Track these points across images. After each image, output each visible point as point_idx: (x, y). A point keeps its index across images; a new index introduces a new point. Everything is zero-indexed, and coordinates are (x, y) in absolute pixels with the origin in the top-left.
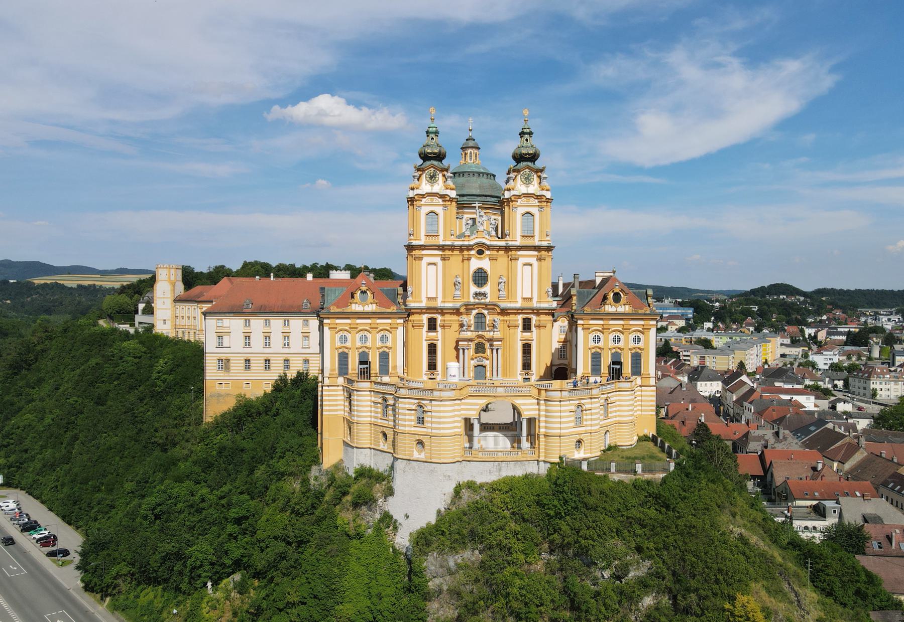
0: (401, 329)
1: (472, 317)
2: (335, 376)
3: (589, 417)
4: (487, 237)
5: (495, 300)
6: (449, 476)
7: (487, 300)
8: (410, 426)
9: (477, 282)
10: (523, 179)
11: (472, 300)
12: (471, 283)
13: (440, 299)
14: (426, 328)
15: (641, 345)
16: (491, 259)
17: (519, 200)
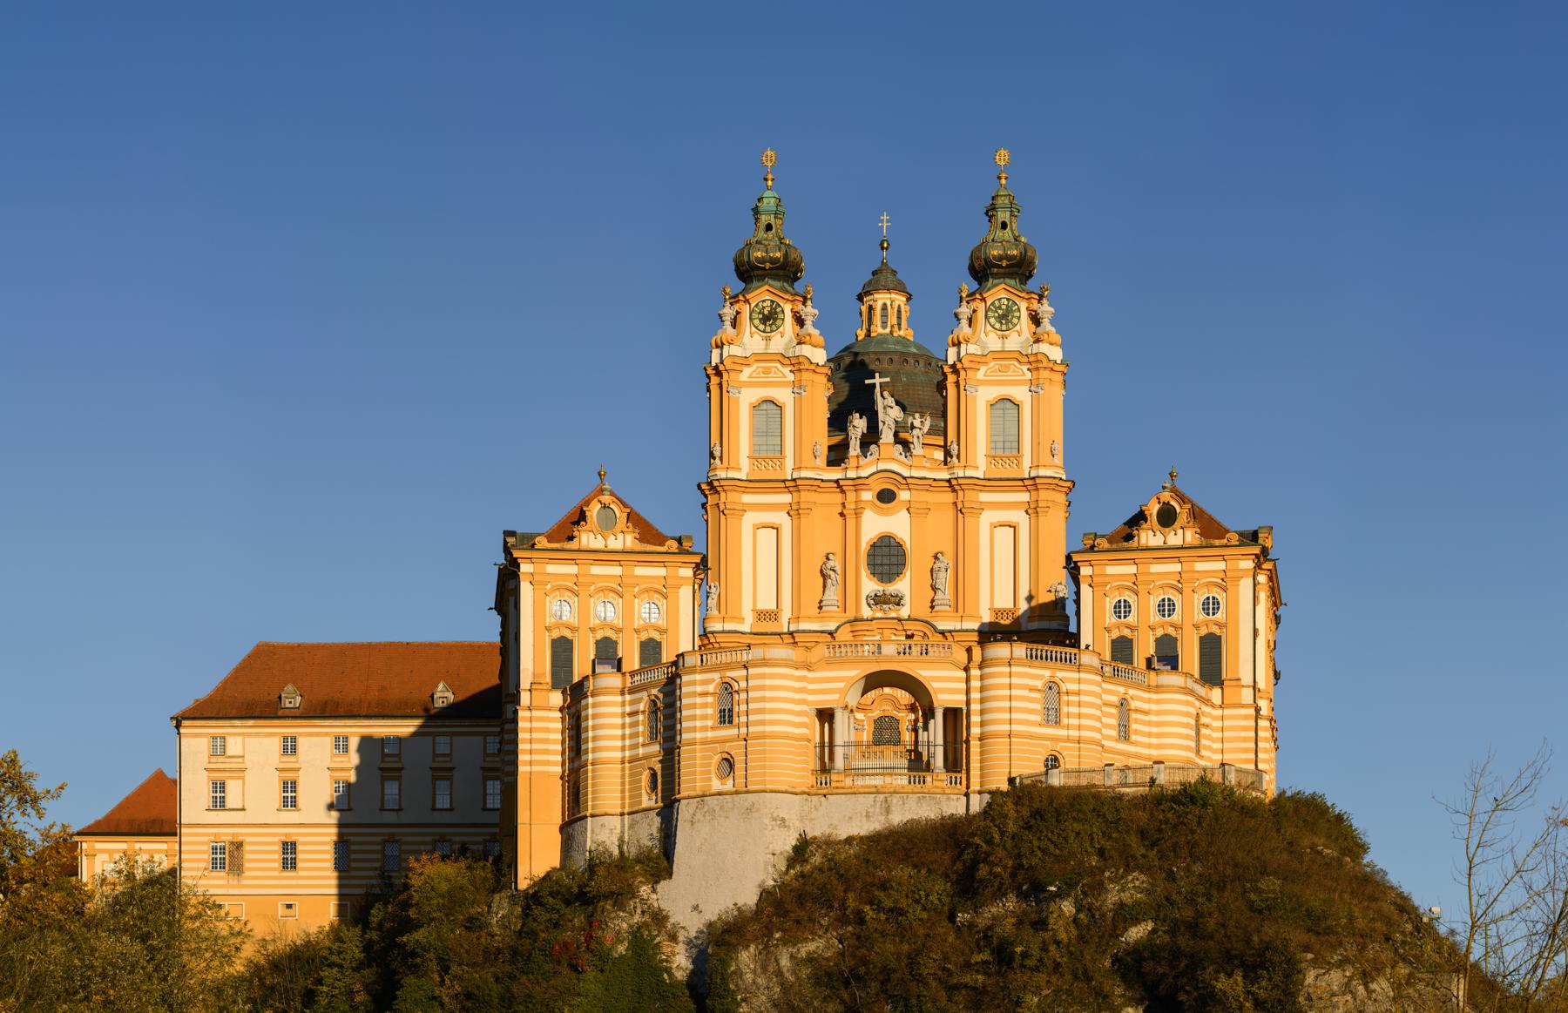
0: (685, 593)
2: (545, 687)
3: (1074, 710)
5: (924, 612)
6: (783, 820)
7: (904, 612)
8: (704, 729)
11: (866, 612)
12: (864, 573)
13: (786, 614)
17: (983, 369)
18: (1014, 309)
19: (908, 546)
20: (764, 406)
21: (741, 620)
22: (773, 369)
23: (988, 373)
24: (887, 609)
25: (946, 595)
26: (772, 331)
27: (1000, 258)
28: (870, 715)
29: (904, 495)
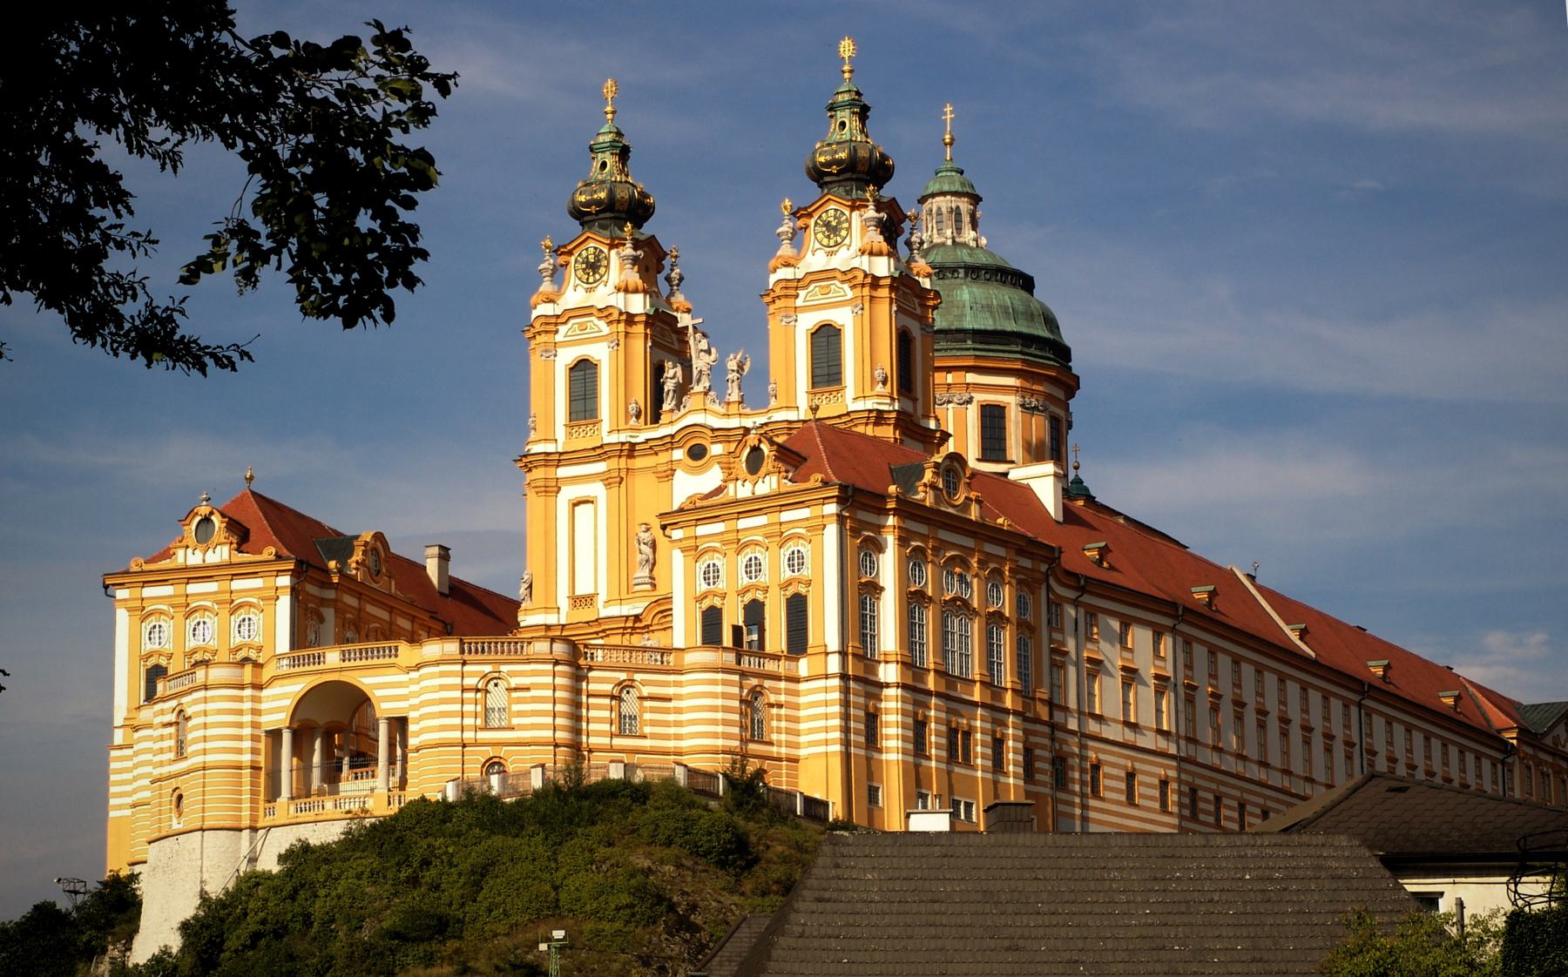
4: (716, 407)
10: (820, 236)
15: (806, 573)
17: (802, 293)
23: (808, 299)
26: (595, 281)
27: (828, 164)
29: (716, 449)
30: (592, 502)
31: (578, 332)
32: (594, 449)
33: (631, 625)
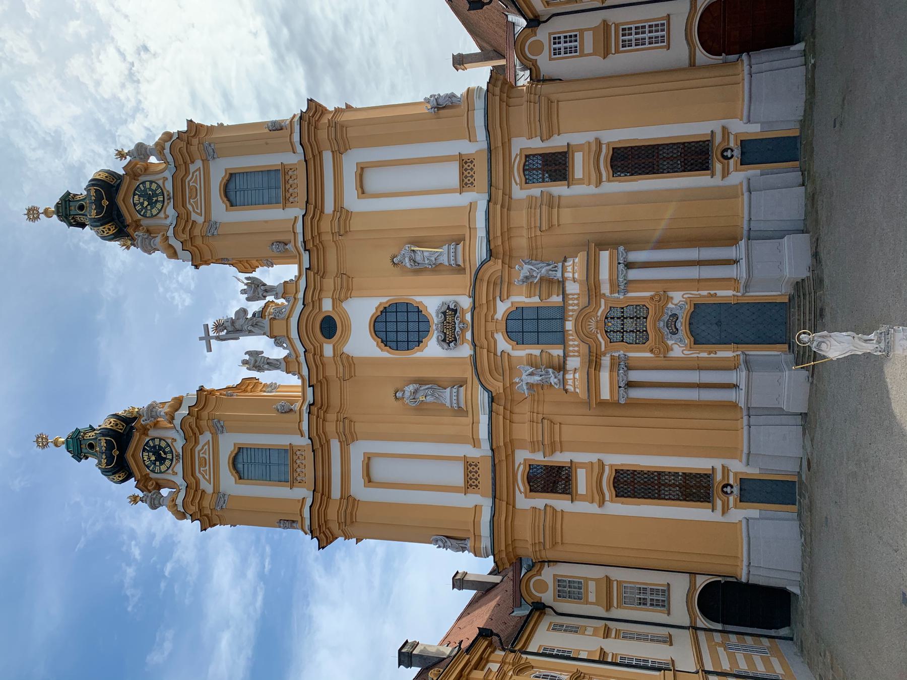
1: (521, 353)
5: (466, 279)
9: (413, 337)
10: (155, 211)
11: (465, 351)
14: (561, 503)
16: (345, 291)
17: (194, 216)
18: (143, 189)
19: (384, 300)
20: (240, 466)
21: (477, 508)
22: (201, 455)
23: (199, 211)
24: (461, 325)
25: (443, 254)
26: (172, 452)
28: (603, 349)
29: (327, 306)
30: (369, 458)
31: (207, 467)
32: (313, 451)
33: (502, 408)
